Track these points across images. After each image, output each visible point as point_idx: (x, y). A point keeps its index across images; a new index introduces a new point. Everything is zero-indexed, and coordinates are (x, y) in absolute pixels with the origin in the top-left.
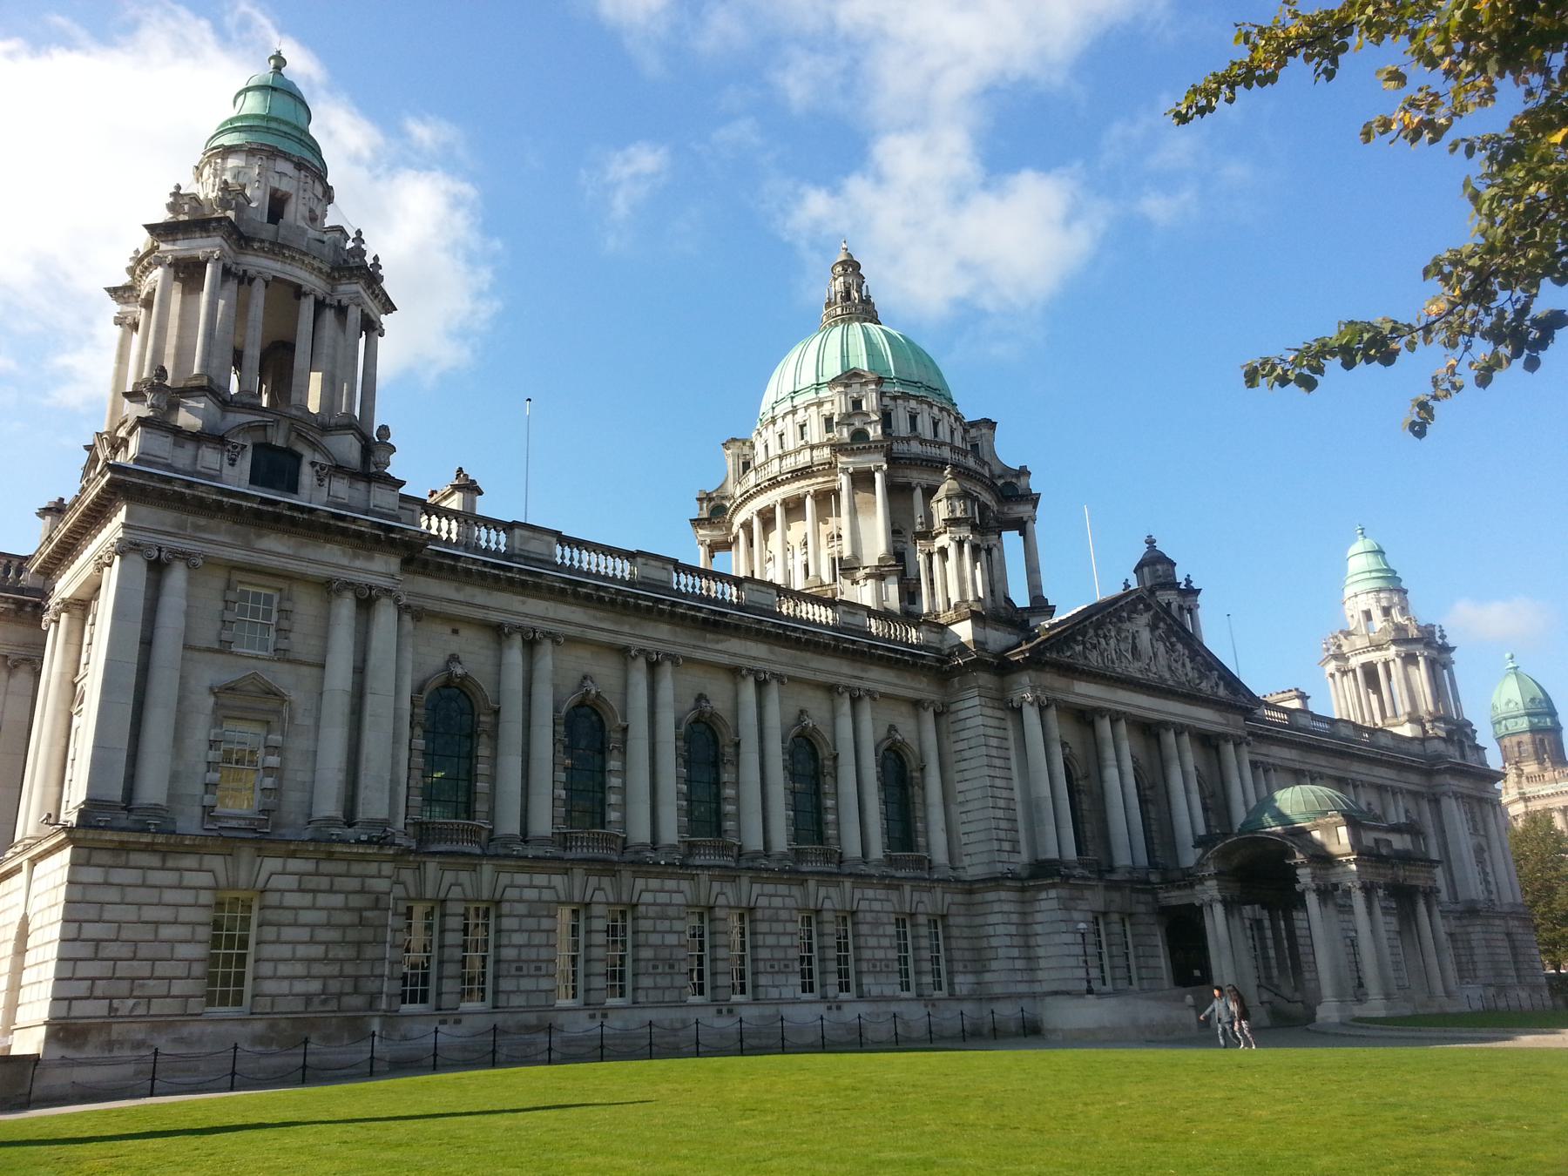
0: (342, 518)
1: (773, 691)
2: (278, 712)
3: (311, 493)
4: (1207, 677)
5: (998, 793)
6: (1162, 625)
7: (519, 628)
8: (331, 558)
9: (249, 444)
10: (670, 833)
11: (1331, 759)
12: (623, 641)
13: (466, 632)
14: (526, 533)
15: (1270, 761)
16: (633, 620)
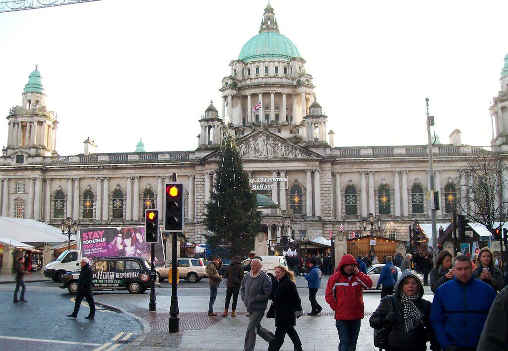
0: (26, 167)
1: (136, 181)
2: (23, 202)
3: (26, 163)
4: (293, 153)
5: (199, 200)
6: (271, 139)
7: (70, 178)
8: (28, 174)
9: (15, 156)
10: (105, 218)
11: (417, 164)
12: (94, 176)
13: (62, 181)
14: (72, 157)
15: (371, 170)
16: (97, 171)
